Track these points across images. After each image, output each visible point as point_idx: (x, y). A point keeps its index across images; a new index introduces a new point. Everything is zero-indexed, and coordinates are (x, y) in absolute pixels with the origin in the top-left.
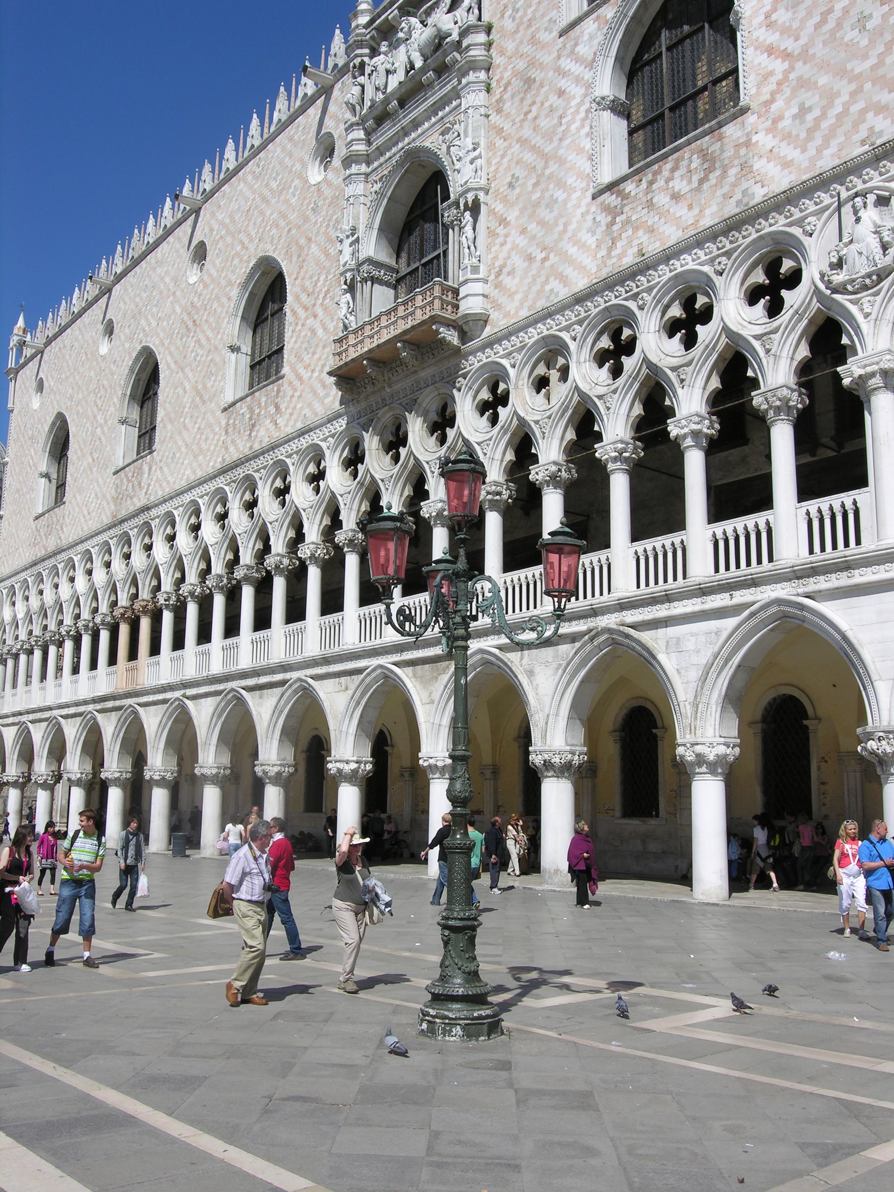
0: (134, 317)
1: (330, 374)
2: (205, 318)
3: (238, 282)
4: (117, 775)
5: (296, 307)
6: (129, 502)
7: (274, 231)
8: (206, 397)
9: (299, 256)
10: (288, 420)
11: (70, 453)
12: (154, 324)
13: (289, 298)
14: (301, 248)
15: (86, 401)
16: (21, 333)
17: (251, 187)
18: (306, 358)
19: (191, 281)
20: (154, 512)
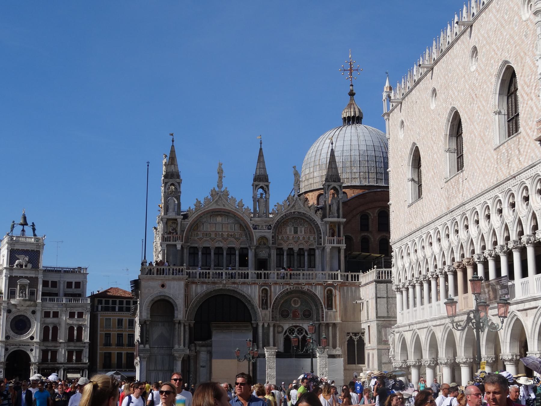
0: (446, 88)
1: (536, 140)
2: (480, 93)
3: (494, 74)
4: (464, 360)
5: (523, 93)
6: (454, 200)
7: (509, 46)
8: (486, 141)
9: (521, 63)
10: (525, 158)
11: (422, 168)
12: (456, 94)
13: (519, 87)
14: (522, 58)
15: (427, 137)
16: (388, 90)
17: (495, 17)
18: (530, 123)
19: (472, 70)
20: (467, 207)
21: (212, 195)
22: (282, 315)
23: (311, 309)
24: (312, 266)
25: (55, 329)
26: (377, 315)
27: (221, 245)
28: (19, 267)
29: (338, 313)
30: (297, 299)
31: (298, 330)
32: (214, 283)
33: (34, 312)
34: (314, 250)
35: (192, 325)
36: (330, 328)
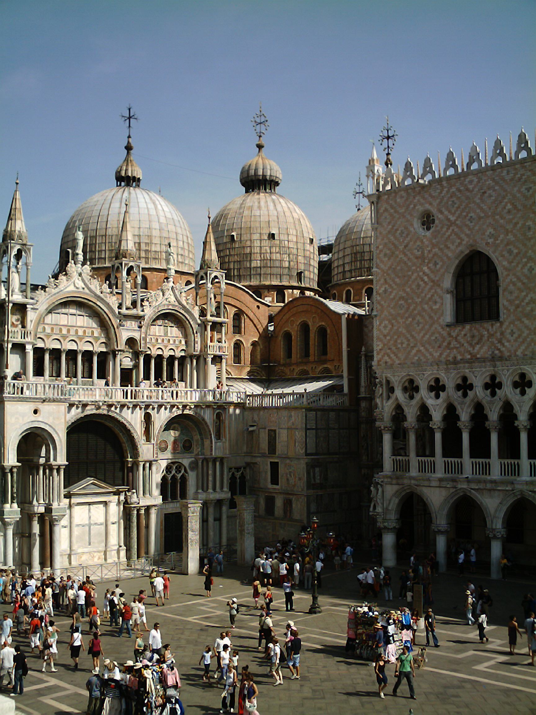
23: (192, 438)
29: (227, 444)
31: (176, 467)
32: (85, 406)
36: (218, 464)
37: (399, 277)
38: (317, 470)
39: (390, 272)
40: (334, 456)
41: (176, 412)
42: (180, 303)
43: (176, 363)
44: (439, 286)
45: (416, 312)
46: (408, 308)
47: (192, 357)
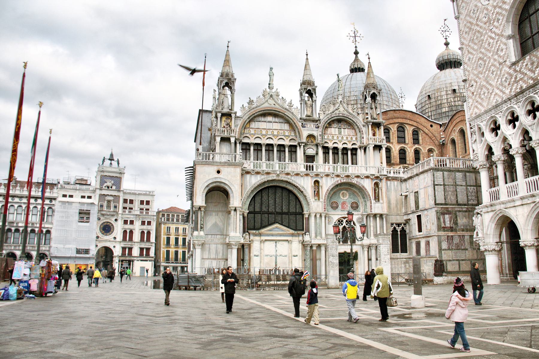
21: (264, 96)
22: (332, 207)
23: (359, 201)
24: (354, 162)
25: (131, 232)
26: (435, 202)
27: (270, 142)
28: (106, 188)
29: (385, 205)
30: (345, 192)
31: (347, 221)
32: (268, 173)
33: (116, 220)
34: (356, 149)
35: (246, 215)
36: (378, 219)
37: (475, 44)
38: (447, 216)
39: (470, 44)
40: (463, 207)
41: (338, 180)
42: (347, 111)
43: (349, 152)
44: (502, 36)
45: (490, 64)
46: (485, 64)
47: (360, 148)
